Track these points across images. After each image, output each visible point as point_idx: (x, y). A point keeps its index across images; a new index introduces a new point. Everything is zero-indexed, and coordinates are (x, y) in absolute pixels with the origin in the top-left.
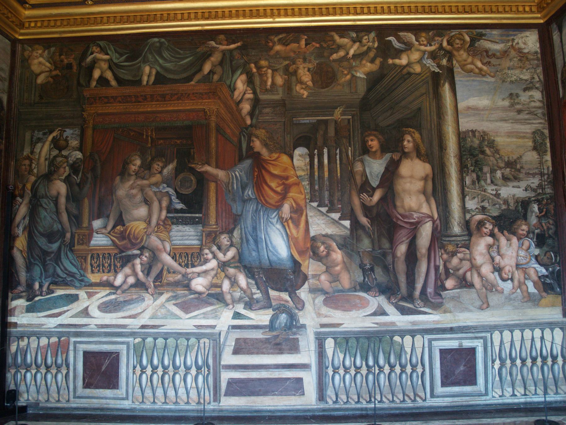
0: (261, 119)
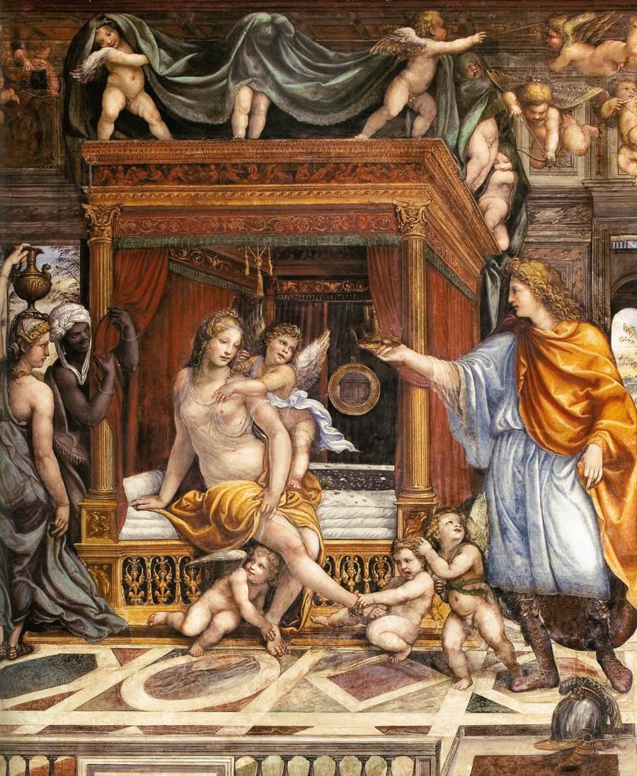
0: (535, 234)
